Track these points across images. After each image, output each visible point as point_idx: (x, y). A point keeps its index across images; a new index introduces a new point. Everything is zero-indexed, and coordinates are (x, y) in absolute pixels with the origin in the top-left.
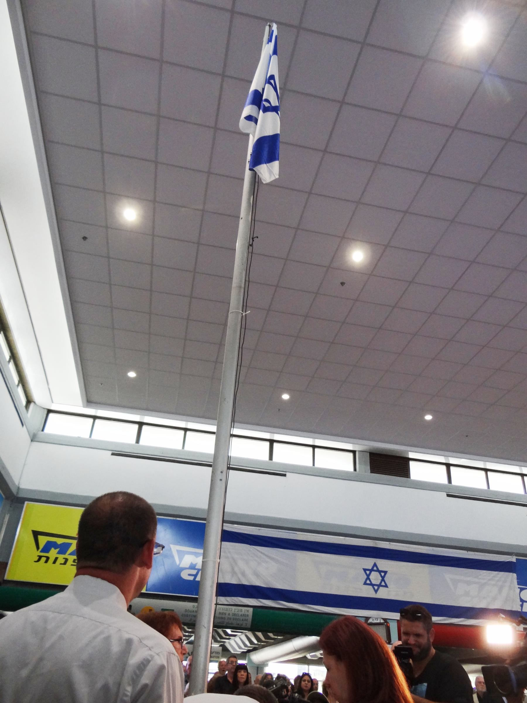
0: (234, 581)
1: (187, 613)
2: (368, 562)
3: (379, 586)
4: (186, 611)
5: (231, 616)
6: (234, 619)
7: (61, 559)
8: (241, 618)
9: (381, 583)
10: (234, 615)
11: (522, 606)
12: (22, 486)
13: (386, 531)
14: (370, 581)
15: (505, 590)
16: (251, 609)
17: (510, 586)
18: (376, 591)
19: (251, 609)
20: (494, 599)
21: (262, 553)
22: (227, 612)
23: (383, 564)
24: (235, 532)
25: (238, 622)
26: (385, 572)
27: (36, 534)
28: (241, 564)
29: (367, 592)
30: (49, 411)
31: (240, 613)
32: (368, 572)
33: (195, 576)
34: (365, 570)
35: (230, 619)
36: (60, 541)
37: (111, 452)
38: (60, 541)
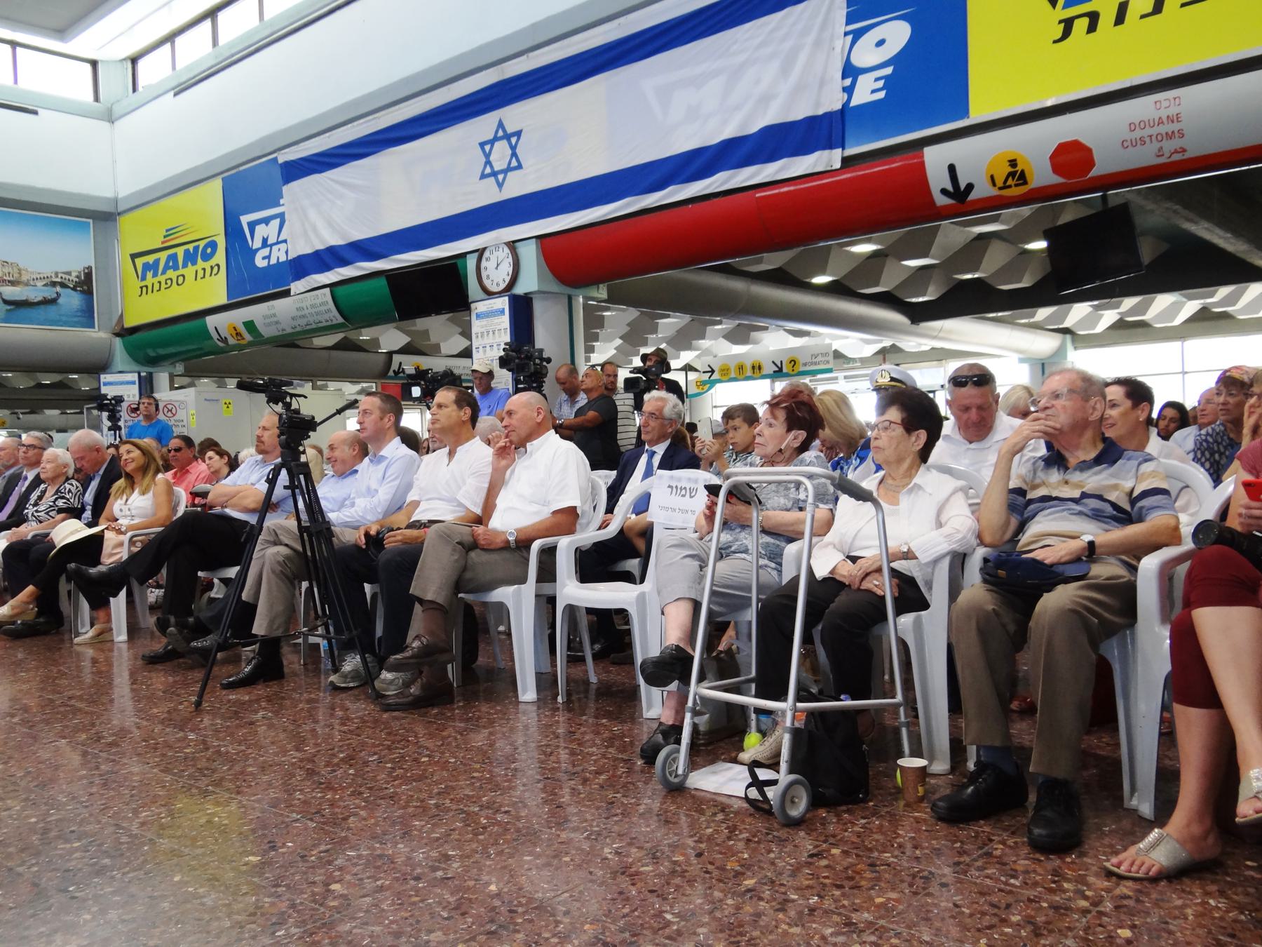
0: (309, 251)
1: (268, 321)
2: (484, 126)
3: (505, 172)
4: (265, 317)
5: (310, 310)
6: (317, 314)
7: (156, 287)
8: (323, 308)
9: (510, 163)
10: (313, 306)
11: (849, 90)
12: (122, 194)
13: (535, 27)
14: (492, 167)
15: (802, 57)
16: (328, 290)
17: (817, 43)
18: (500, 185)
19: (328, 290)
20: (765, 99)
21: (337, 182)
22: (304, 305)
23: (515, 115)
24: (302, 159)
25: (319, 318)
26: (518, 134)
27: (134, 256)
28: (313, 215)
29: (486, 195)
30: (134, 61)
31: (318, 302)
32: (486, 146)
33: (268, 257)
34: (482, 145)
35: (311, 314)
36: (150, 259)
37: (172, 93)
38: (150, 259)
